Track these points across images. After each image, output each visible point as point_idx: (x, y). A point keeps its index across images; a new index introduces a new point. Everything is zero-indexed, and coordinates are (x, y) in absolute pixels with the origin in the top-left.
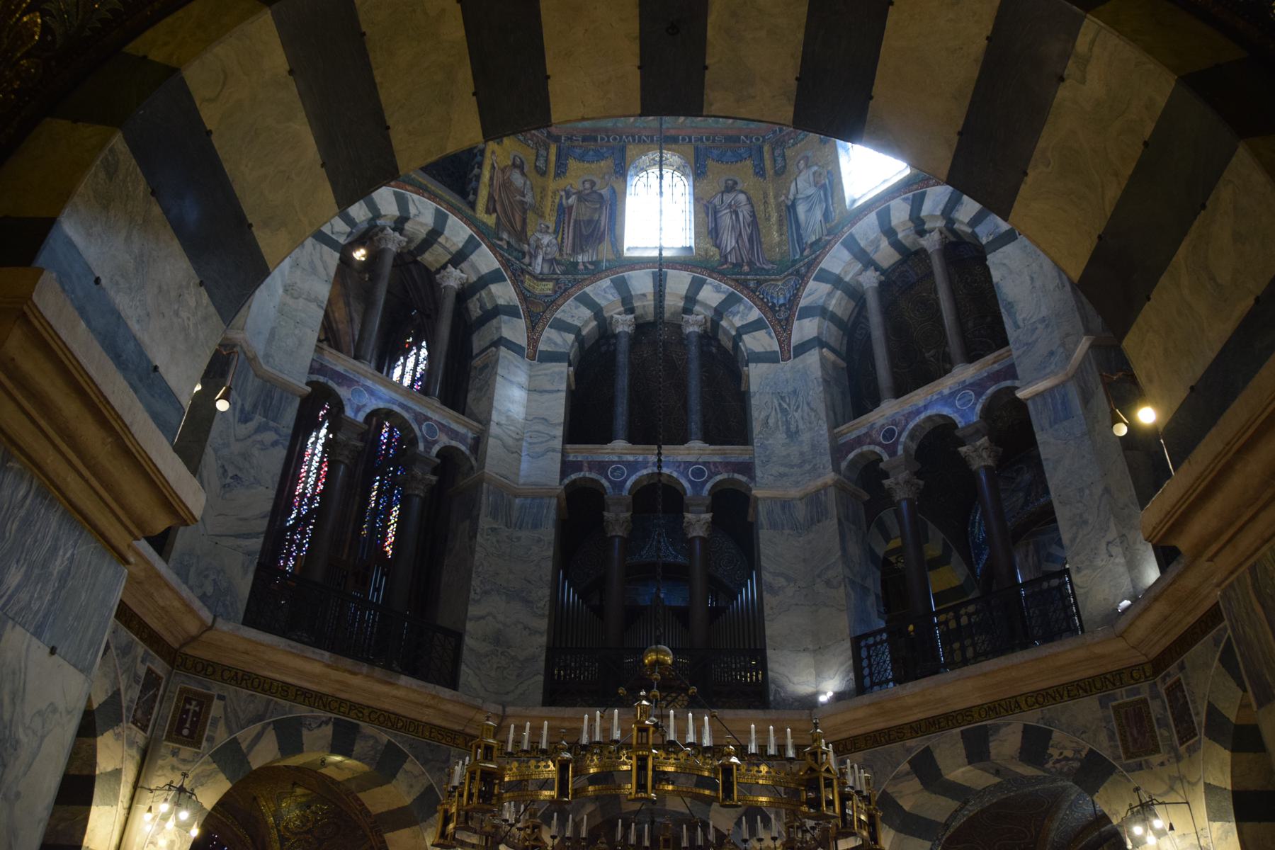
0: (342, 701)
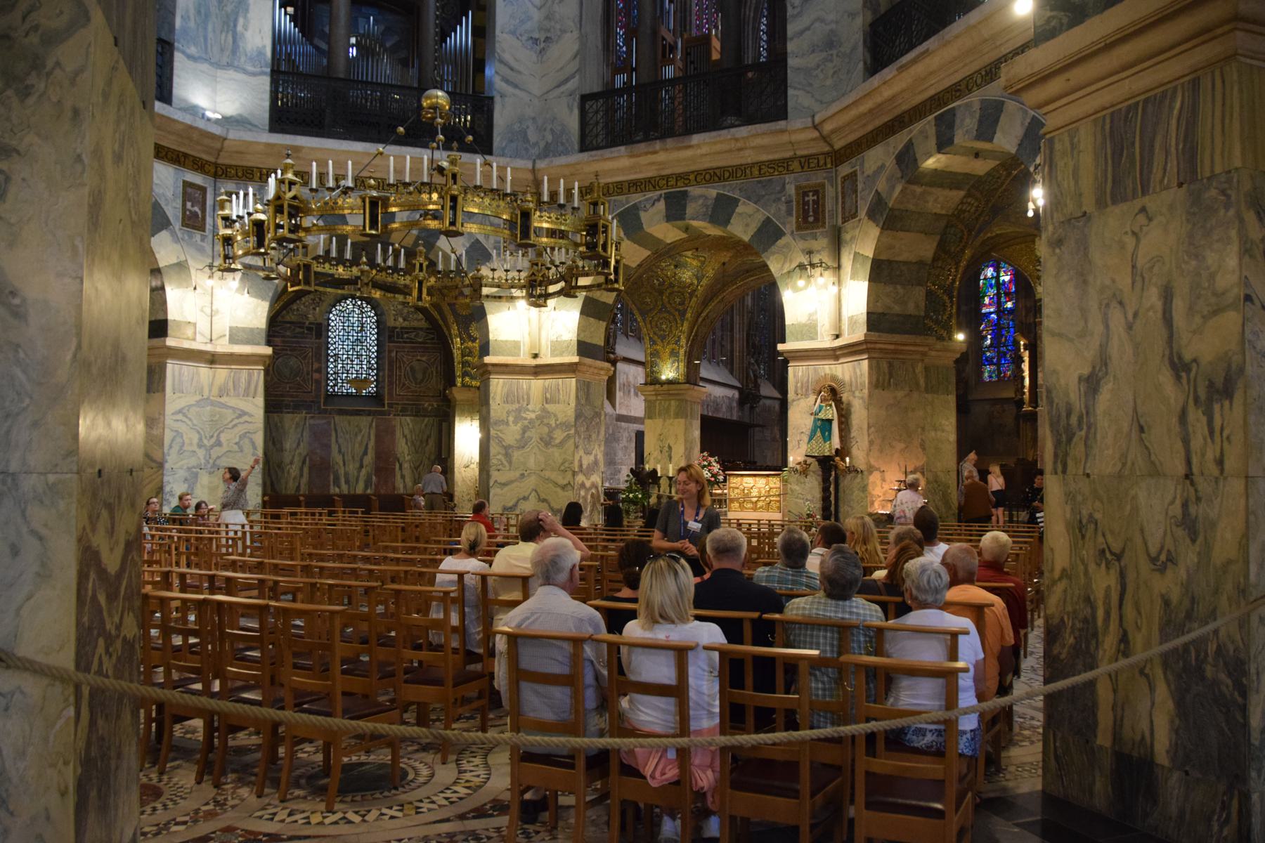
0: (668, 177)
